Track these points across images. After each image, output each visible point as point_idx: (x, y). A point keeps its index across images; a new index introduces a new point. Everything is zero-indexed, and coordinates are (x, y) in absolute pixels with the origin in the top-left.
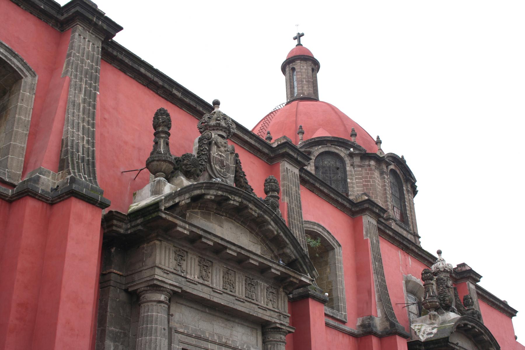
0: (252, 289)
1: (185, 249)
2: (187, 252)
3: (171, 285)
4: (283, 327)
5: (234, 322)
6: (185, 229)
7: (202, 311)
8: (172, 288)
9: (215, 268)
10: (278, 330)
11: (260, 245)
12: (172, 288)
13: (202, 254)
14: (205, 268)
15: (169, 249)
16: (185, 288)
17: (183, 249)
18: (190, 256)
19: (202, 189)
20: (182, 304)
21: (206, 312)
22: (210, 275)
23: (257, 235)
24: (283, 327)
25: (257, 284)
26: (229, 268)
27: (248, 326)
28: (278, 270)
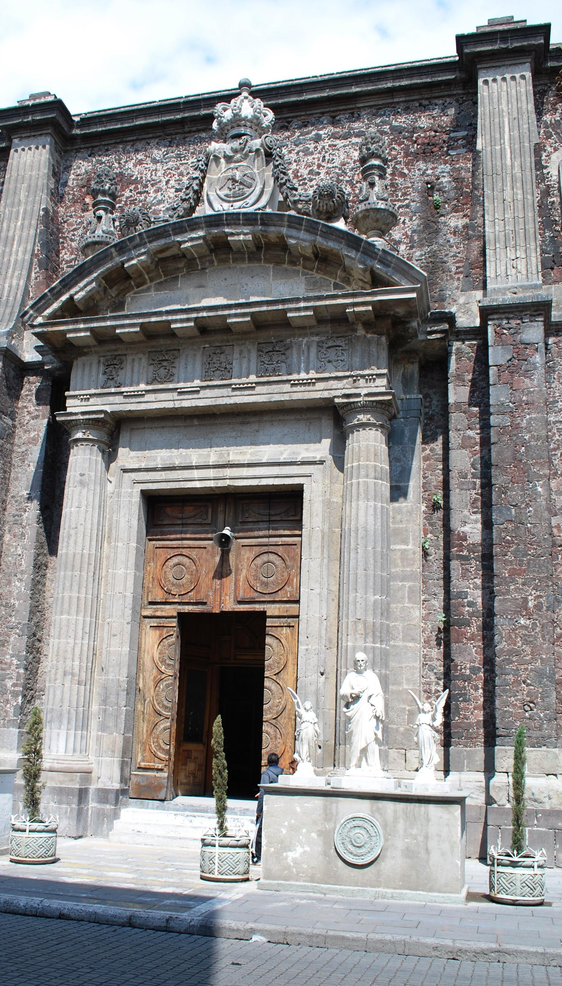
0: (275, 358)
1: (120, 353)
2: (126, 355)
3: (83, 413)
4: (352, 400)
5: (259, 422)
6: (80, 330)
7: (185, 427)
8: (87, 417)
9: (184, 355)
10: (349, 408)
11: (304, 274)
12: (87, 417)
13: (153, 347)
14: (165, 364)
15: (91, 364)
16: (108, 409)
17: (116, 353)
18: (130, 358)
19: (112, 258)
20: (144, 428)
21: (193, 426)
22: (174, 371)
23: (293, 263)
24: (352, 400)
25: (289, 347)
26: (217, 344)
27: (298, 420)
28: (306, 309)
